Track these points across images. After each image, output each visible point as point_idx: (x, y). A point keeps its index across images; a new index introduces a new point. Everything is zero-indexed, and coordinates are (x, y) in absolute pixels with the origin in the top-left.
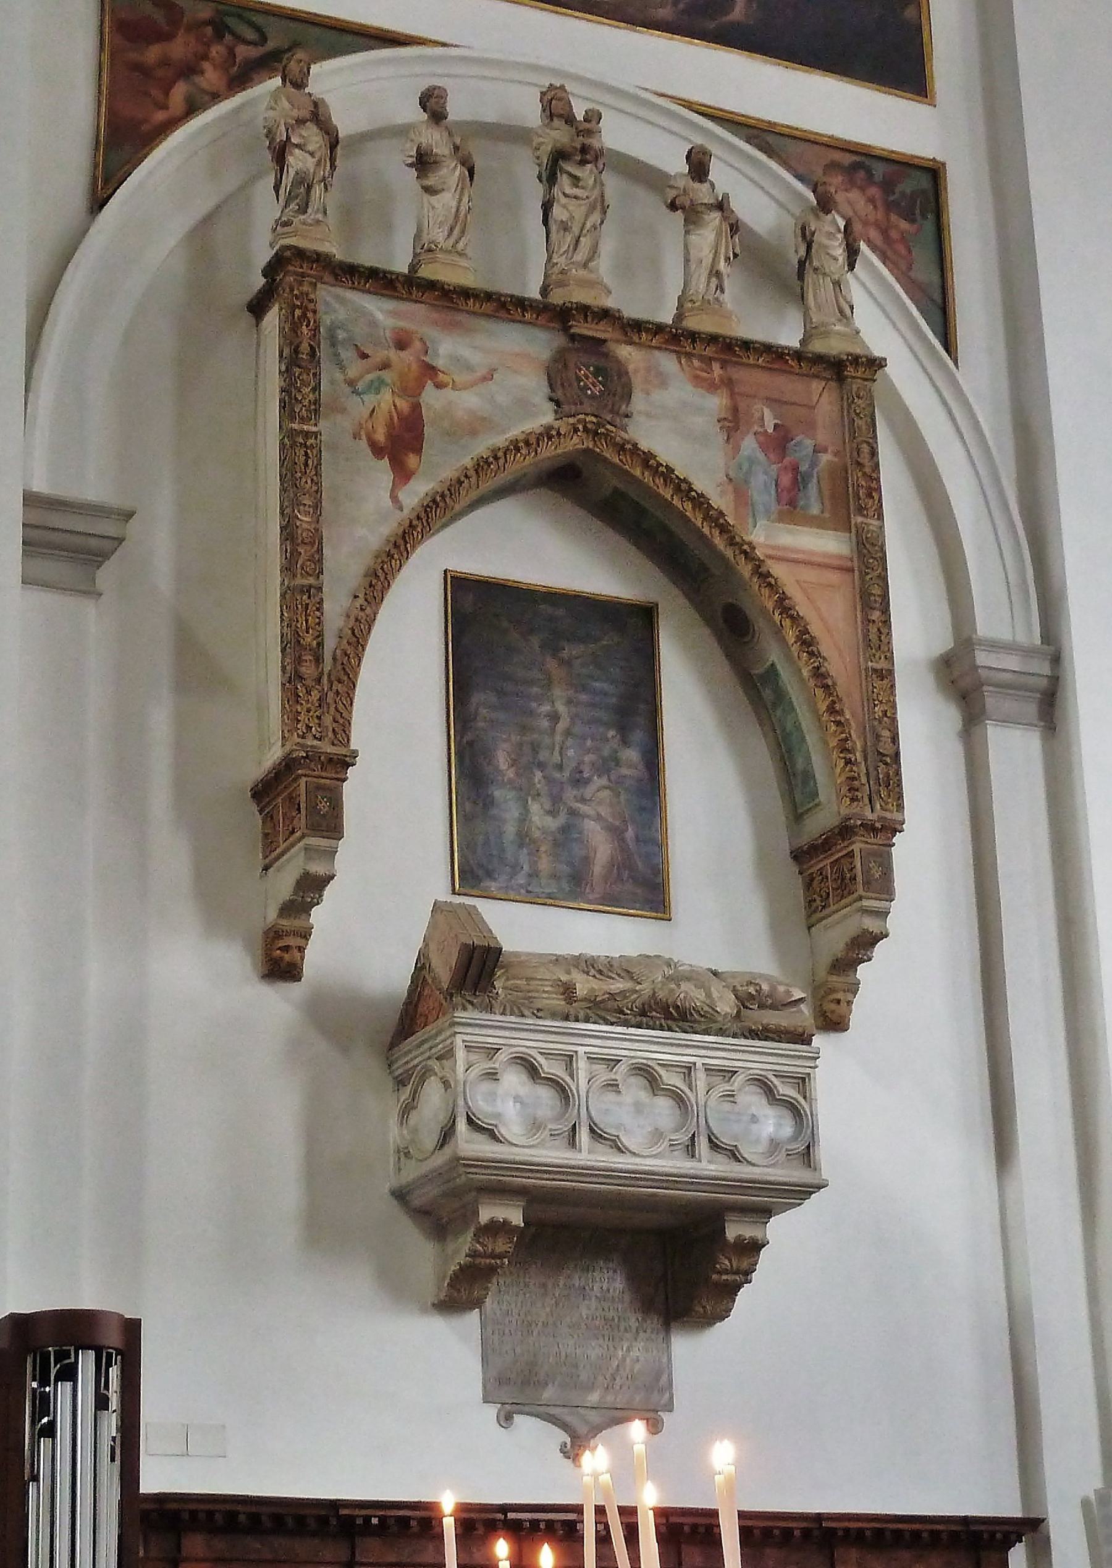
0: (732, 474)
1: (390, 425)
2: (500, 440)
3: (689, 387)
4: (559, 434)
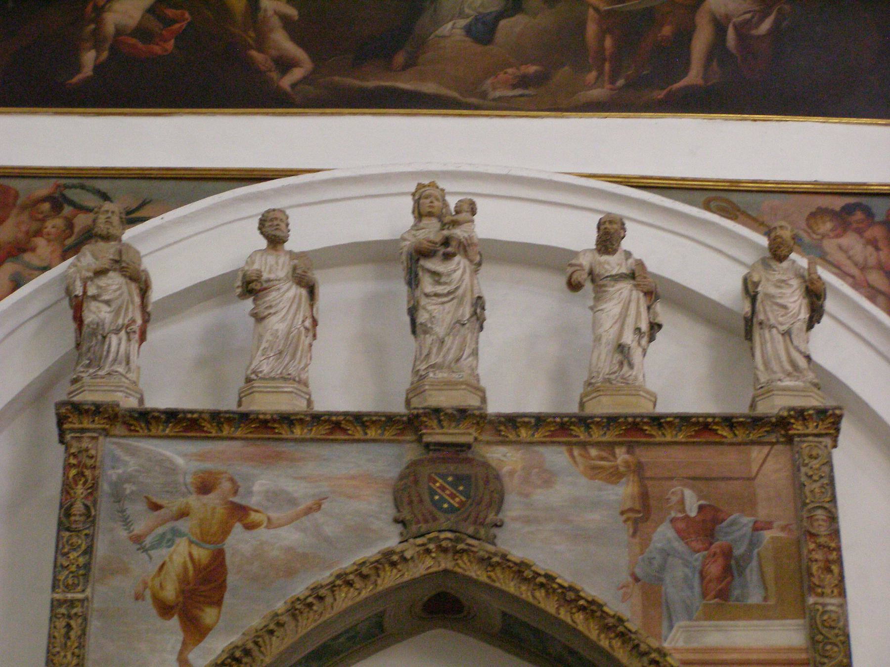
0: (639, 572)
1: (183, 580)
2: (325, 576)
3: (583, 480)
4: (404, 560)
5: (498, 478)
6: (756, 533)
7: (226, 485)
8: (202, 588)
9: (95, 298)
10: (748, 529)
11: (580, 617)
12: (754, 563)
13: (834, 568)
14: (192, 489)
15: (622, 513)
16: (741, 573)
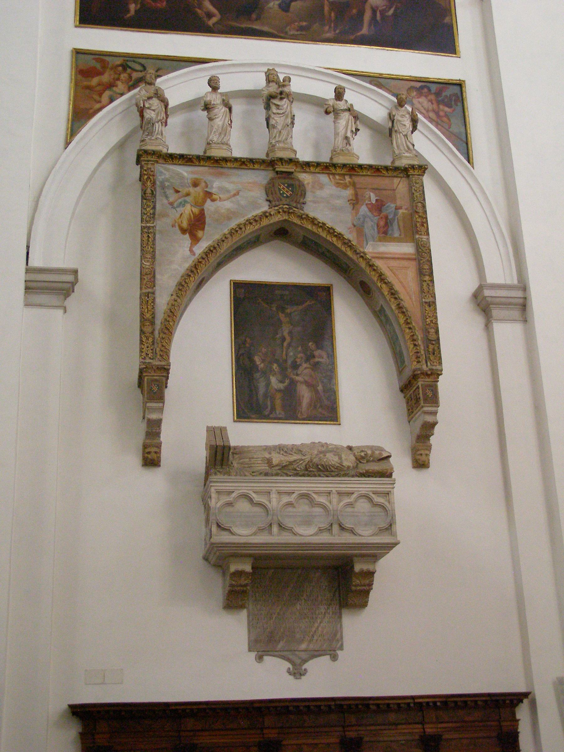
0: (355, 223)
1: (190, 220)
2: (242, 220)
3: (334, 188)
4: (271, 215)
5: (303, 185)
6: (397, 210)
7: (203, 184)
8: (197, 223)
9: (149, 108)
10: (393, 209)
11: (334, 239)
12: (396, 221)
13: (425, 225)
14: (191, 185)
15: (348, 201)
16: (392, 224)
